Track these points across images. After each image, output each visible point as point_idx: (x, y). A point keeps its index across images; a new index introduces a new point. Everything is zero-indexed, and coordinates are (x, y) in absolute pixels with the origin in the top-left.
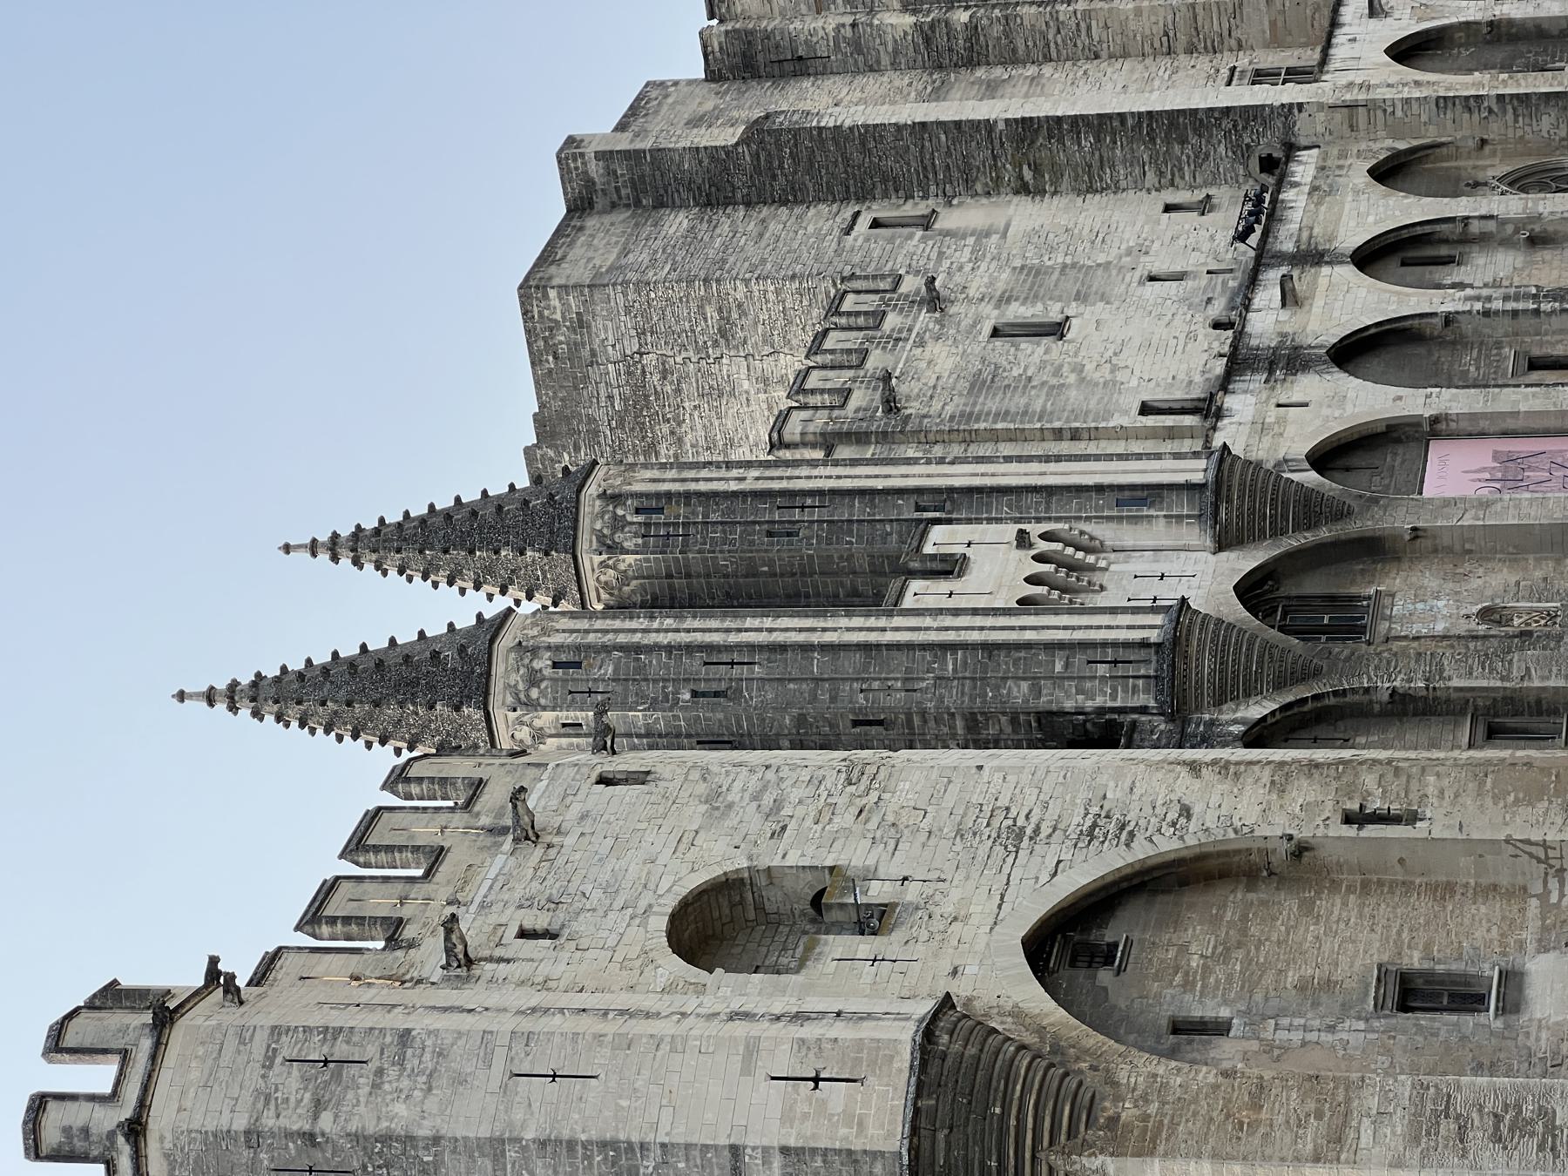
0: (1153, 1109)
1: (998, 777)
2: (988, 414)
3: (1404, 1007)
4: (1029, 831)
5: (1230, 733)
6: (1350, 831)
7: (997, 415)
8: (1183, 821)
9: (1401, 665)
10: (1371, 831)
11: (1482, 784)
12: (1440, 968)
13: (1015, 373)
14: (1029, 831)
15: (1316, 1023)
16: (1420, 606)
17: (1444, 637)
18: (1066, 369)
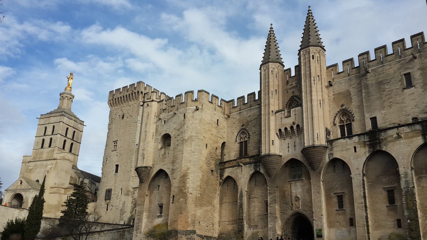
0: (143, 188)
1: (182, 156)
2: (368, 90)
3: (160, 206)
4: (174, 163)
5: (257, 169)
6: (171, 196)
7: (368, 91)
8: (174, 179)
9: (273, 188)
10: (171, 199)
11: (177, 209)
12: (163, 209)
13: (387, 87)
14: (174, 163)
15: (158, 199)
16: (299, 187)
17: (291, 192)
18: (389, 96)
